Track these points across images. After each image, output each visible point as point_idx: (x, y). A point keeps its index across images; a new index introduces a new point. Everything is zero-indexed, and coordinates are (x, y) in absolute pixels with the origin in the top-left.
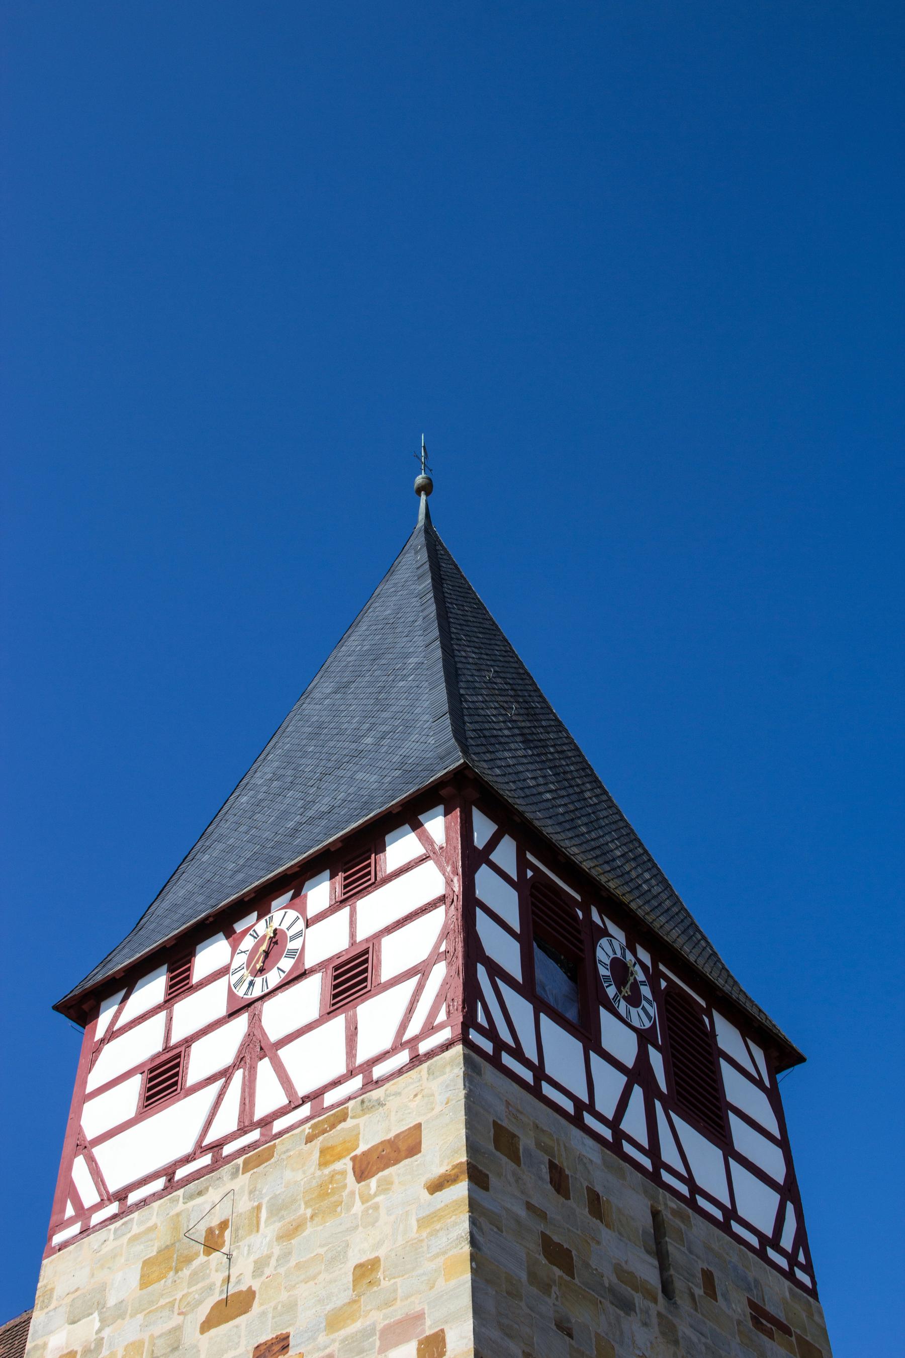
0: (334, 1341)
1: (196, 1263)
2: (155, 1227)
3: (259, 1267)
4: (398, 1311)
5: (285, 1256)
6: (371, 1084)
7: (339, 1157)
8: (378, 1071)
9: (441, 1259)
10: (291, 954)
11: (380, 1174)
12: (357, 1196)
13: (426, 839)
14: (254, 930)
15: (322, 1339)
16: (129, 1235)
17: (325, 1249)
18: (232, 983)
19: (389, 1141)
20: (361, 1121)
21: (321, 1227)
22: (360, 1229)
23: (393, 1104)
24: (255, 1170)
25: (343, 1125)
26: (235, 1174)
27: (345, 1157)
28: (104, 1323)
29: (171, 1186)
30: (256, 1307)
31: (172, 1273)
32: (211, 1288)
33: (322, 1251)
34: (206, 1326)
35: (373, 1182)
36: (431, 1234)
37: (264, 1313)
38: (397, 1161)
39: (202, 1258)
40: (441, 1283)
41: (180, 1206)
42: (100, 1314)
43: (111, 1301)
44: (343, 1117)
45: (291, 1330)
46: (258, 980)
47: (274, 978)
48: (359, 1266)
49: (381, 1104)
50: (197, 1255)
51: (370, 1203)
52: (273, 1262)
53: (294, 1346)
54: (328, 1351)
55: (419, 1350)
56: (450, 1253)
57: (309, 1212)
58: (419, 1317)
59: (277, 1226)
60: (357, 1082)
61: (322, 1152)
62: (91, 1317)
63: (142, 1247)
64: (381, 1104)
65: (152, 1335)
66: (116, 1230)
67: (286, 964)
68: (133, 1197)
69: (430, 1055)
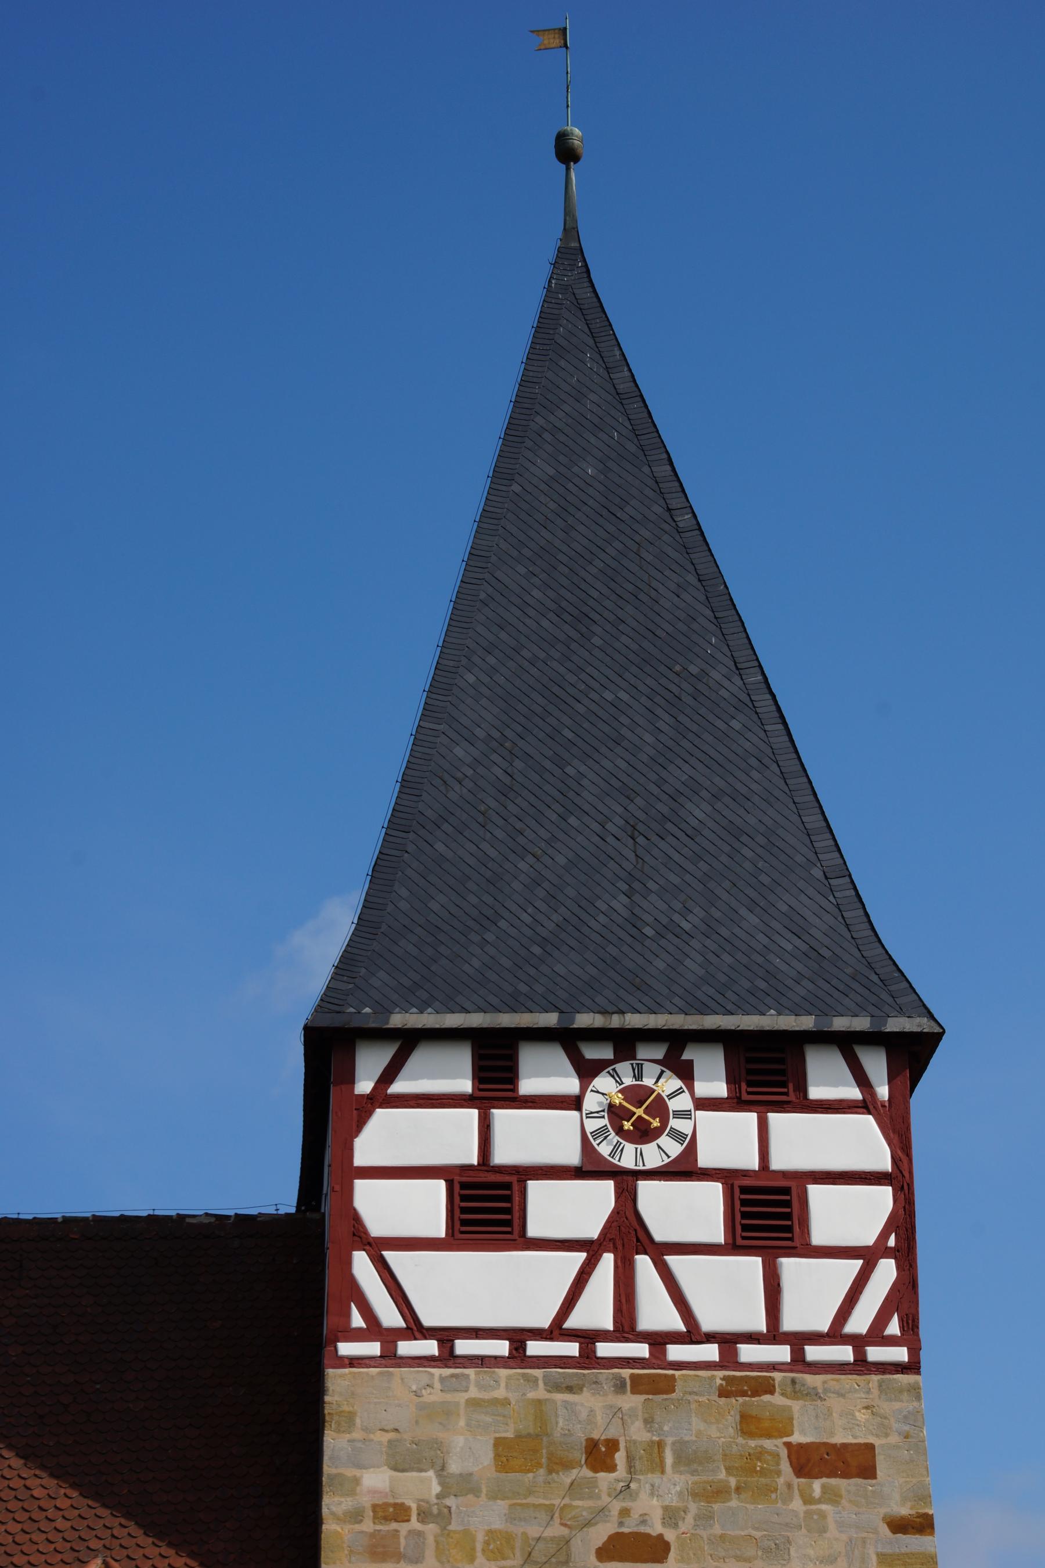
2: (506, 1402)
3: (671, 1516)
5: (705, 1518)
7: (769, 1436)
8: (814, 1353)
10: (677, 1136)
11: (824, 1480)
12: (796, 1492)
14: (614, 1070)
16: (465, 1396)
19: (834, 1446)
20: (796, 1406)
21: (752, 1507)
22: (803, 1530)
23: (834, 1403)
24: (650, 1397)
25: (766, 1398)
26: (620, 1387)
27: (776, 1437)
29: (518, 1356)
31: (542, 1471)
33: (757, 1534)
34: (605, 1553)
38: (846, 1475)
44: (771, 1391)
46: (629, 1148)
47: (653, 1156)
49: (813, 1395)
51: (814, 1507)
52: (690, 1519)
57: (733, 1482)
59: (692, 1479)
60: (782, 1353)
62: (423, 1474)
63: (488, 1419)
64: (813, 1395)
65: (524, 1534)
66: (442, 1379)
67: (676, 1149)
68: (463, 1347)
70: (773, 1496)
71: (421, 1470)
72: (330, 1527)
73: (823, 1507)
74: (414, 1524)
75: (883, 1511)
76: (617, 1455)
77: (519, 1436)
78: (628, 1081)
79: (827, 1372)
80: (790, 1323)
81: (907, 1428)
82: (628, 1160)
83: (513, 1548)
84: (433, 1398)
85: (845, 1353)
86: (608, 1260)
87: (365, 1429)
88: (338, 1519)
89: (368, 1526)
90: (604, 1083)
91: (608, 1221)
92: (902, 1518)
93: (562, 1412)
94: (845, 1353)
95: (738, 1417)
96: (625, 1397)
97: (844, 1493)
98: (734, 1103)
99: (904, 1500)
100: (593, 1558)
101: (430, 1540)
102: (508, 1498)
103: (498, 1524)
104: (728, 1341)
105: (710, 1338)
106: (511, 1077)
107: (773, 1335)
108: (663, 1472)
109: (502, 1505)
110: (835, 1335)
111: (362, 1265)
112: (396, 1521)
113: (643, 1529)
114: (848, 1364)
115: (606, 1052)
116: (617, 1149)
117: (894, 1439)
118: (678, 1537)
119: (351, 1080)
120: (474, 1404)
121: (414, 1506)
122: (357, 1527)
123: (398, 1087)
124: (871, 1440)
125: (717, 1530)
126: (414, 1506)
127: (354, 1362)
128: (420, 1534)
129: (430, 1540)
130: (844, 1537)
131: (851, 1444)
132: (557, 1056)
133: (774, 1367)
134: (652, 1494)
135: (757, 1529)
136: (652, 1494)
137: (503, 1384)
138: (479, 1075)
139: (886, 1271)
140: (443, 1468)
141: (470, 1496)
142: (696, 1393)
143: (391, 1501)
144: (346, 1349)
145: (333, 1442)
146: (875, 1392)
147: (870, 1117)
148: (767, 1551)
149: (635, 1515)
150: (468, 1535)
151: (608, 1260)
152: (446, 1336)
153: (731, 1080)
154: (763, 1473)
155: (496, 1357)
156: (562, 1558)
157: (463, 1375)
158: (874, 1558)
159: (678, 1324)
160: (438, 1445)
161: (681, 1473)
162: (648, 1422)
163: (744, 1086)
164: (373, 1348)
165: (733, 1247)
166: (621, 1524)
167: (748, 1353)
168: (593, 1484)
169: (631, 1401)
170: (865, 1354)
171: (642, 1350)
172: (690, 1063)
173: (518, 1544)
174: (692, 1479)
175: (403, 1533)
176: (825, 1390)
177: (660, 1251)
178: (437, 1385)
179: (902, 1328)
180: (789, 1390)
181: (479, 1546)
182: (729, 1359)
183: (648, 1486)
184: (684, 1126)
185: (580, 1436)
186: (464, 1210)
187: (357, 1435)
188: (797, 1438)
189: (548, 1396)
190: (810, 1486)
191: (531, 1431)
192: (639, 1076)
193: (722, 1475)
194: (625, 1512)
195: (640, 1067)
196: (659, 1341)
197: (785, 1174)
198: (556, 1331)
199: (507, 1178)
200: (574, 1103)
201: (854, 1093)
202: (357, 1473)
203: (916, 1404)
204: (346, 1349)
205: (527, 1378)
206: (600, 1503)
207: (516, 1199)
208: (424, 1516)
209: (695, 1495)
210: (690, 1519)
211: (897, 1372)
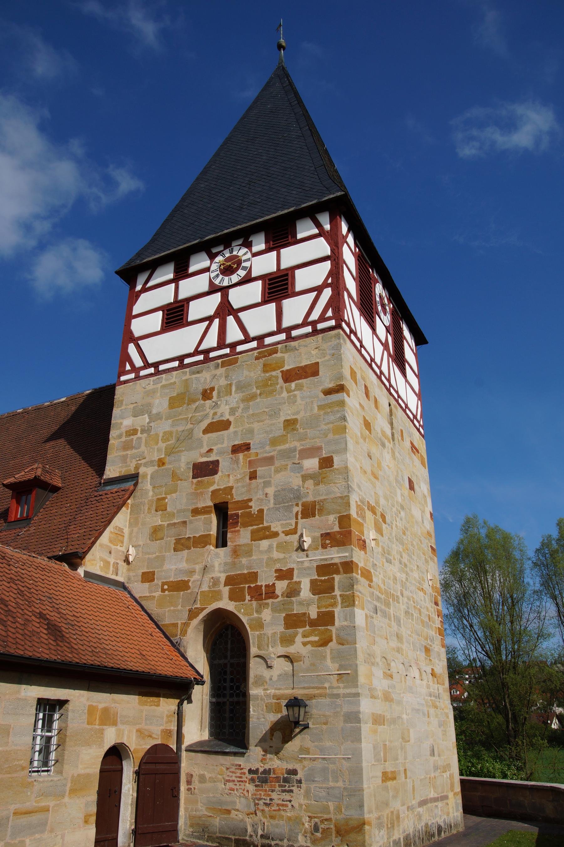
0: (275, 450)
1: (197, 403)
2: (175, 383)
3: (233, 411)
4: (308, 444)
5: (247, 408)
6: (290, 338)
8: (294, 333)
9: (331, 426)
10: (244, 268)
11: (297, 381)
12: (284, 389)
13: (318, 225)
14: (223, 253)
15: (267, 448)
16: (161, 384)
17: (268, 410)
18: (212, 277)
19: (301, 367)
20: (286, 356)
21: (266, 400)
22: (287, 404)
23: (303, 350)
24: (228, 367)
26: (217, 367)
27: (277, 370)
28: (151, 420)
29: (182, 366)
30: (232, 429)
31: (185, 405)
32: (206, 416)
33: (266, 410)
34: (205, 431)
35: (293, 385)
36: (325, 413)
37: (235, 432)
38: (306, 377)
39: (202, 402)
40: (331, 436)
41: (188, 376)
42: (149, 416)
43: (154, 411)
44: (276, 353)
45: (252, 442)
46: (226, 278)
47: (235, 278)
48: (286, 421)
49: (295, 349)
50: (198, 400)
51: (292, 394)
52: (240, 410)
53: (252, 449)
54: (271, 454)
55: (319, 462)
56: (335, 424)
57: (258, 392)
58: (320, 448)
59: (241, 395)
60: (283, 336)
61: (265, 365)
62: (144, 416)
63: (168, 391)
64: (295, 349)
65: (177, 430)
66: (153, 381)
67: (242, 273)
68: (162, 367)
69: (324, 331)
70: (275, 393)
71: (143, 415)
72: (111, 442)
73: (295, 393)
74: (139, 435)
75: (321, 388)
76: (214, 393)
77: (178, 395)
78: (227, 255)
79: (300, 339)
80: (286, 324)
81: (333, 352)
82: (226, 283)
83: (172, 437)
84: (151, 388)
85: (309, 329)
86: (217, 321)
87: (126, 405)
88: (115, 439)
89: (124, 439)
90: (219, 259)
91: (217, 307)
92: (330, 389)
93: (195, 382)
94: (309, 329)
95: (262, 366)
96: (218, 370)
97: (305, 384)
98: (268, 250)
99: (331, 381)
100: (201, 434)
101: (144, 440)
102: (172, 418)
103: (167, 429)
104: (260, 339)
105: (254, 339)
106: (187, 266)
107: (280, 330)
108: (231, 395)
109: (170, 421)
110: (305, 324)
111: (132, 349)
112: (133, 435)
113: (221, 419)
114: (309, 333)
115: (221, 248)
116: (222, 280)
117: (328, 357)
118: (235, 419)
119: (135, 287)
120: (164, 387)
121: (139, 429)
122: (120, 440)
123: (150, 284)
124: (318, 361)
125: (251, 412)
126: (139, 429)
127: (126, 382)
128: (140, 438)
129: (144, 440)
130: (304, 402)
131: (309, 364)
132: (204, 255)
133: (278, 343)
134: (226, 404)
135: (267, 408)
136: (226, 404)
137: (174, 377)
138: (176, 271)
139: (327, 293)
140: (150, 413)
141: (159, 421)
142: (246, 361)
143: (132, 428)
144: (123, 378)
145: (116, 412)
146: (320, 341)
147: (322, 238)
148: (270, 416)
149: (219, 414)
150: (157, 435)
151: (217, 321)
152: (156, 365)
153: (266, 242)
154: (271, 385)
155: (173, 368)
156: (190, 437)
157: (161, 377)
158: (316, 408)
159: (243, 338)
160: (150, 405)
161: (238, 393)
162: (226, 377)
163: (272, 243)
164: (132, 376)
165: (265, 301)
166: (213, 418)
167: (268, 341)
168: (204, 406)
169: (221, 371)
170: (316, 327)
171: (227, 351)
172: (251, 241)
173: (174, 435)
174: (241, 395)
175: (135, 439)
176: (299, 346)
177: (235, 312)
178: (152, 383)
179: (333, 312)
180: (284, 350)
181: (160, 438)
182: (261, 345)
183: (225, 402)
184: (247, 264)
185: (201, 388)
186: (167, 319)
187: (123, 408)
188: (286, 368)
189: (190, 377)
190: (290, 386)
191: (183, 392)
192: (231, 252)
193: (254, 390)
194: (215, 414)
195: (232, 249)
196: (233, 346)
197: (287, 269)
198: (196, 352)
199: (182, 303)
200: (207, 270)
201: (316, 231)
202: (121, 421)
203: (338, 341)
204: (123, 378)
205: (183, 373)
206: (206, 412)
207: (185, 310)
208: (143, 431)
209: (243, 401)
210: (240, 410)
211: (330, 331)
